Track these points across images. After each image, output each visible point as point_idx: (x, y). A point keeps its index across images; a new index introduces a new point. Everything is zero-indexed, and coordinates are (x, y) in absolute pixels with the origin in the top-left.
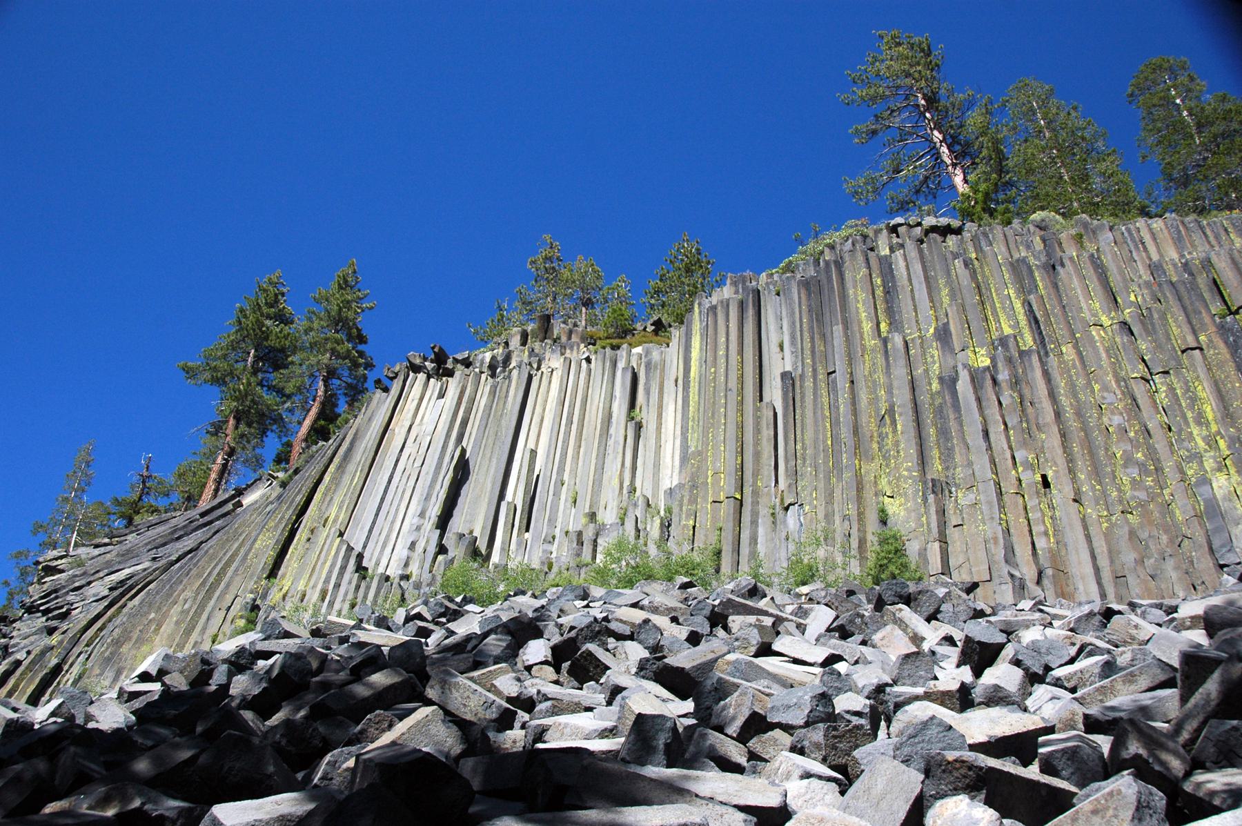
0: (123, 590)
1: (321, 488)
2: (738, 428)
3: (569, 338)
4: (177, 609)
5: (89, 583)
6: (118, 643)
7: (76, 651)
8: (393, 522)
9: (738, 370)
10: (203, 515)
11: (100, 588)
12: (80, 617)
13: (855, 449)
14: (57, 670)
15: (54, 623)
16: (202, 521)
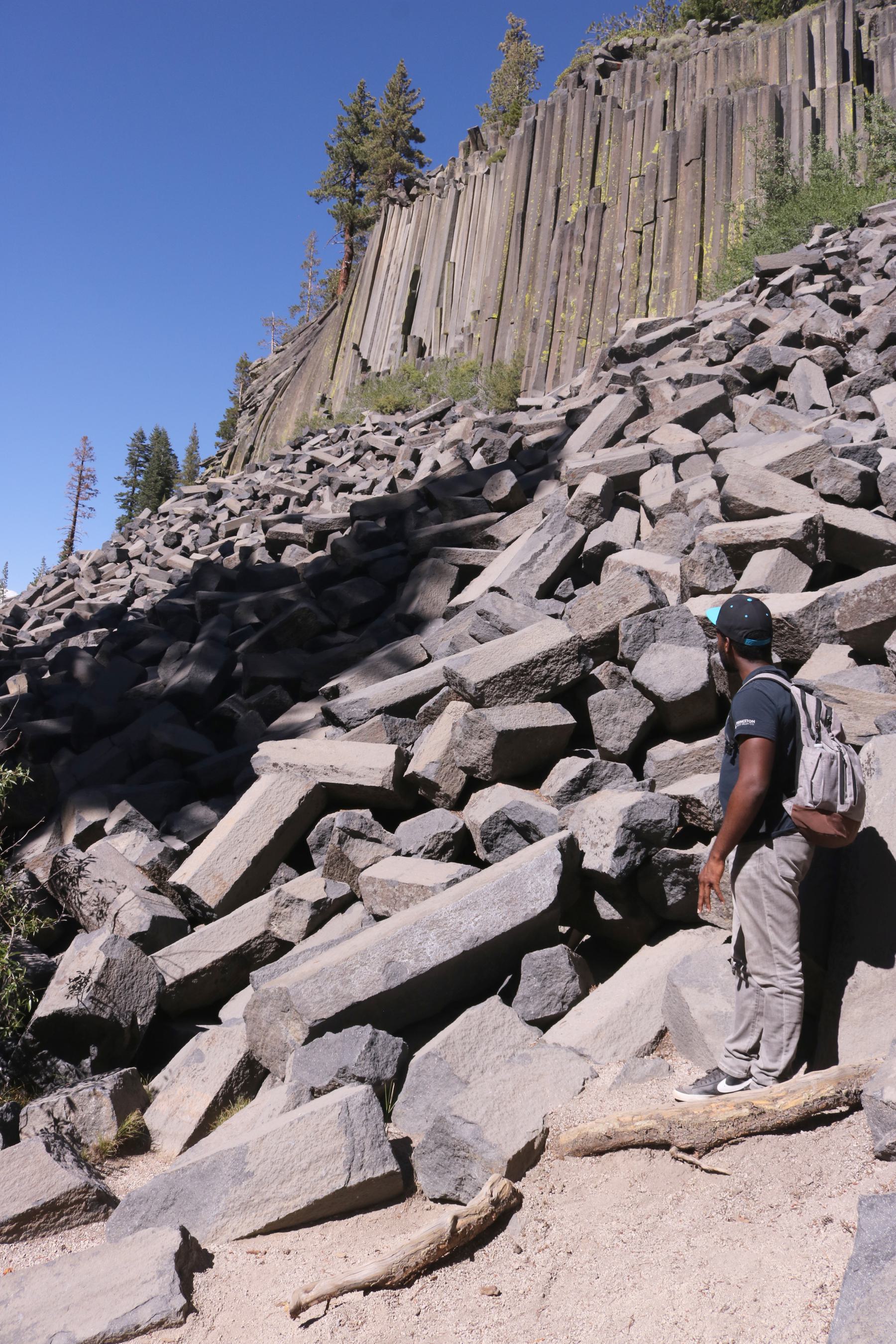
0: (279, 389)
1: (352, 307)
2: (502, 258)
3: (496, 143)
4: (298, 402)
5: (266, 386)
6: (275, 429)
7: (259, 435)
8: (383, 331)
9: (510, 205)
10: (320, 323)
11: (270, 390)
12: (261, 409)
13: (528, 285)
14: (252, 449)
15: (252, 416)
16: (320, 327)
